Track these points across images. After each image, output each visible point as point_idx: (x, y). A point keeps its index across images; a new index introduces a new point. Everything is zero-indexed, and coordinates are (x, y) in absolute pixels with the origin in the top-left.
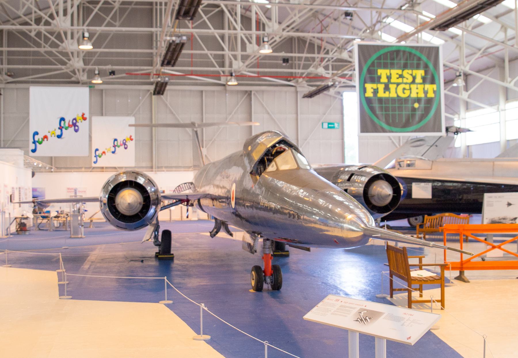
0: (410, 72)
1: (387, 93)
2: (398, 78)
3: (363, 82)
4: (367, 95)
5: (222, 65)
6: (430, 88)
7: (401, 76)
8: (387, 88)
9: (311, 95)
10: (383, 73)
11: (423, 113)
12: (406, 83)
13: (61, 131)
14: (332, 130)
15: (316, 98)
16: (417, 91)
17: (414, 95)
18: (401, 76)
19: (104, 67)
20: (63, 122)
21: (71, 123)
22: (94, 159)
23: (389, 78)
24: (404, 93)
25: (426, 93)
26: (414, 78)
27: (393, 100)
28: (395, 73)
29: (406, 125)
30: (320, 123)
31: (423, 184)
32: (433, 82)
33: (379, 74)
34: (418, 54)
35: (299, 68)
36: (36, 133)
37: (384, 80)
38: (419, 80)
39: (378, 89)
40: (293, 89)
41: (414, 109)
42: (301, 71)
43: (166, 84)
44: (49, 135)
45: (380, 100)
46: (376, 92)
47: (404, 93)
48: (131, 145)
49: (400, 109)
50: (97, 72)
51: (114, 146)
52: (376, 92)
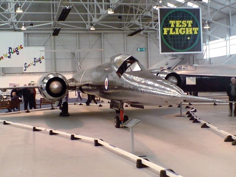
0: (185, 21)
1: (174, 32)
2: (179, 25)
3: (163, 27)
4: (164, 34)
5: (86, 20)
6: (196, 29)
7: (181, 24)
8: (174, 30)
9: (132, 35)
10: (172, 22)
11: (192, 42)
12: (183, 27)
13: (10, 54)
14: (142, 52)
15: (134, 36)
16: (189, 31)
17: (187, 33)
18: (181, 24)
19: (27, 22)
20: (10, 50)
21: (15, 50)
22: (24, 69)
23: (175, 25)
24: (182, 32)
25: (193, 32)
26: (188, 25)
27: (177, 35)
28: (178, 22)
29: (183, 48)
30: (136, 48)
31: (191, 78)
32: (197, 26)
33: (170, 23)
34: (189, 12)
35: (125, 21)
37: (173, 26)
38: (190, 25)
39: (169, 30)
40: (122, 32)
41: (187, 40)
42: (126, 22)
43: (59, 30)
44: (4, 57)
45: (171, 36)
46: (169, 32)
47: (182, 32)
48: (43, 61)
49: (181, 40)
50: (23, 24)
51: (35, 62)
52: (169, 32)
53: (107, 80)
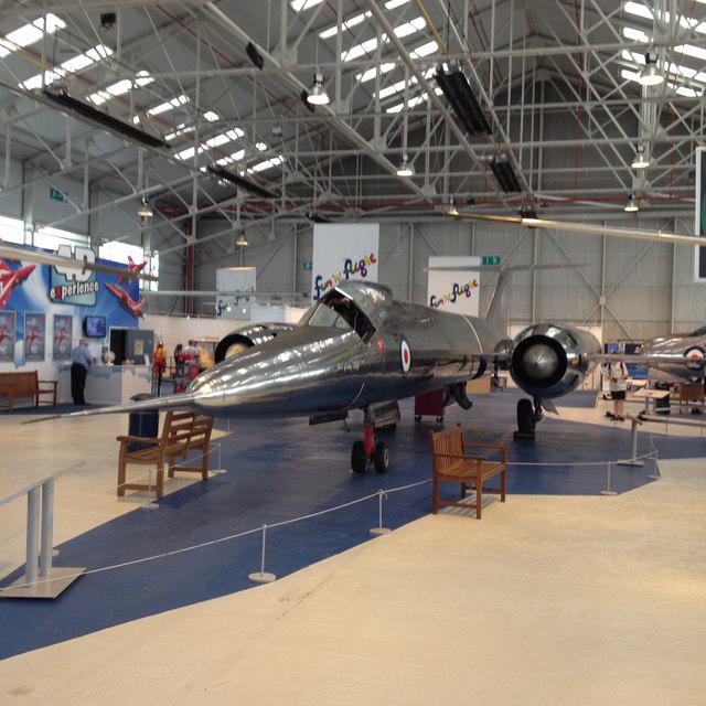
5: (629, 184)
20: (348, 266)
36: (319, 278)
48: (475, 292)
50: (452, 201)
51: (454, 293)
53: (404, 346)
